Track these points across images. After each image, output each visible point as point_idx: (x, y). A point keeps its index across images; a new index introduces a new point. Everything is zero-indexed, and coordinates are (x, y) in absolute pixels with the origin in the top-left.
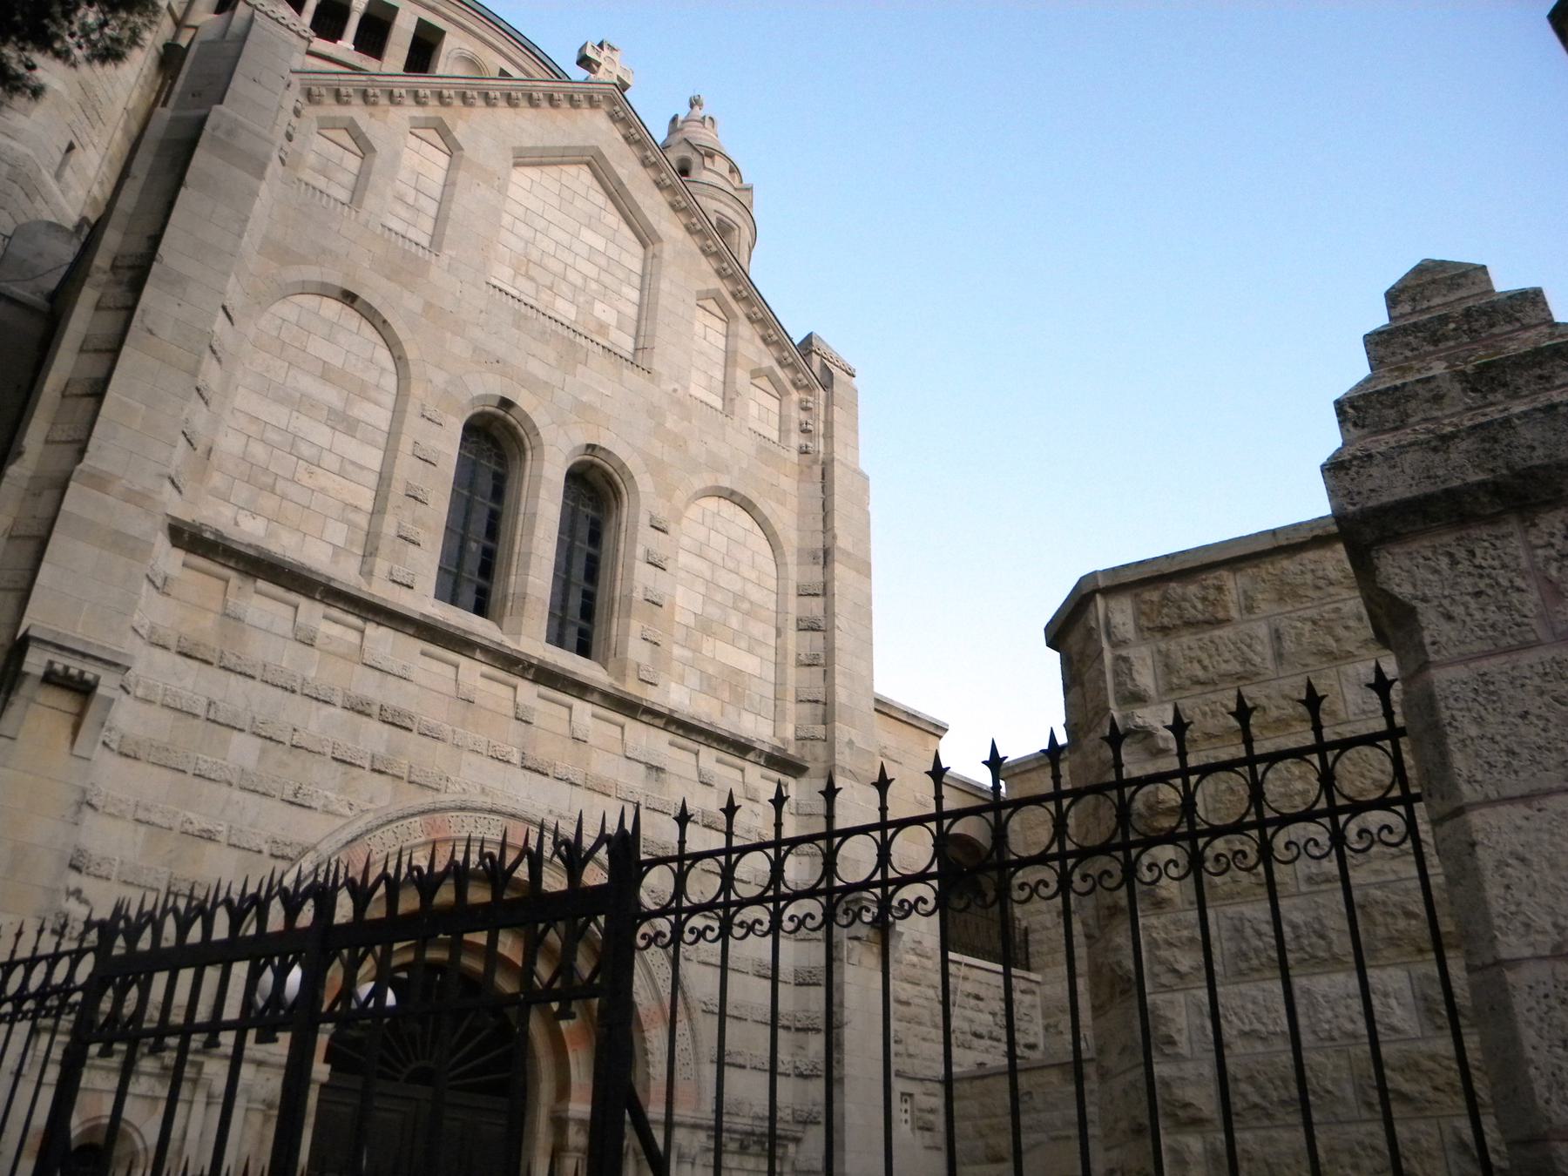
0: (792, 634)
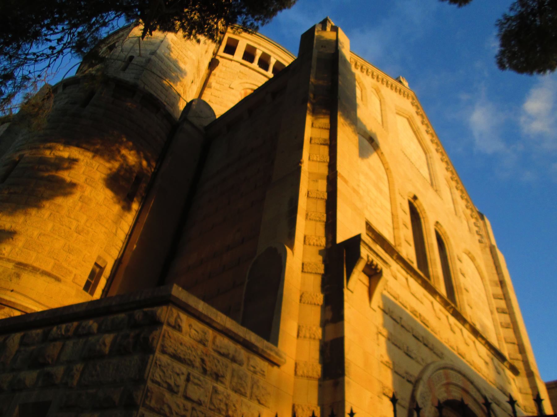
0: (497, 315)
